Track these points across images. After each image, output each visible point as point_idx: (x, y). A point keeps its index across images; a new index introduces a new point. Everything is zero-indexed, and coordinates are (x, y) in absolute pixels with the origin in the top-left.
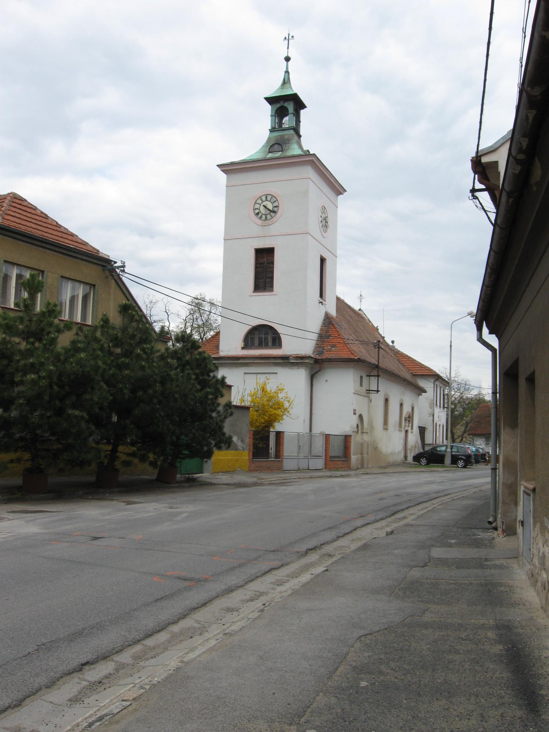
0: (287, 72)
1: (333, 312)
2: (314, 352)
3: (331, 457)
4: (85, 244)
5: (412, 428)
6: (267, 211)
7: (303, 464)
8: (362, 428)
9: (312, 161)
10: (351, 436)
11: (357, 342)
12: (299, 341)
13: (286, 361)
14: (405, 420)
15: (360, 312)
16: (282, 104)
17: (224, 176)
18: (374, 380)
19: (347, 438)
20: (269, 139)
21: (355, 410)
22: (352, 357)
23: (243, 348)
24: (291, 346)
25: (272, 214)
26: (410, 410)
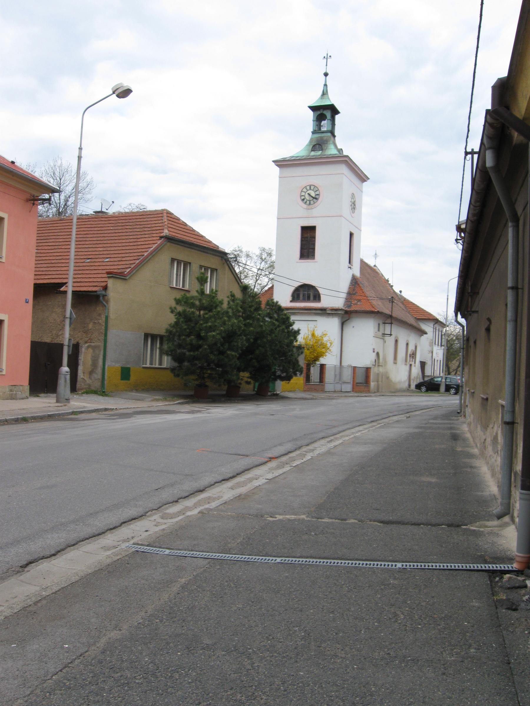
0: (325, 85)
1: (358, 274)
2: (344, 305)
3: (357, 383)
4: (210, 242)
5: (415, 363)
6: (311, 198)
7: (338, 387)
8: (379, 363)
9: (346, 161)
10: (370, 368)
11: (376, 299)
12: (334, 297)
13: (323, 312)
14: (410, 356)
15: (375, 268)
16: (321, 111)
17: (278, 169)
18: (388, 327)
19: (368, 370)
20: (311, 139)
21: (374, 349)
22: (373, 310)
23: (291, 301)
24: (328, 301)
25: (314, 200)
26: (414, 348)
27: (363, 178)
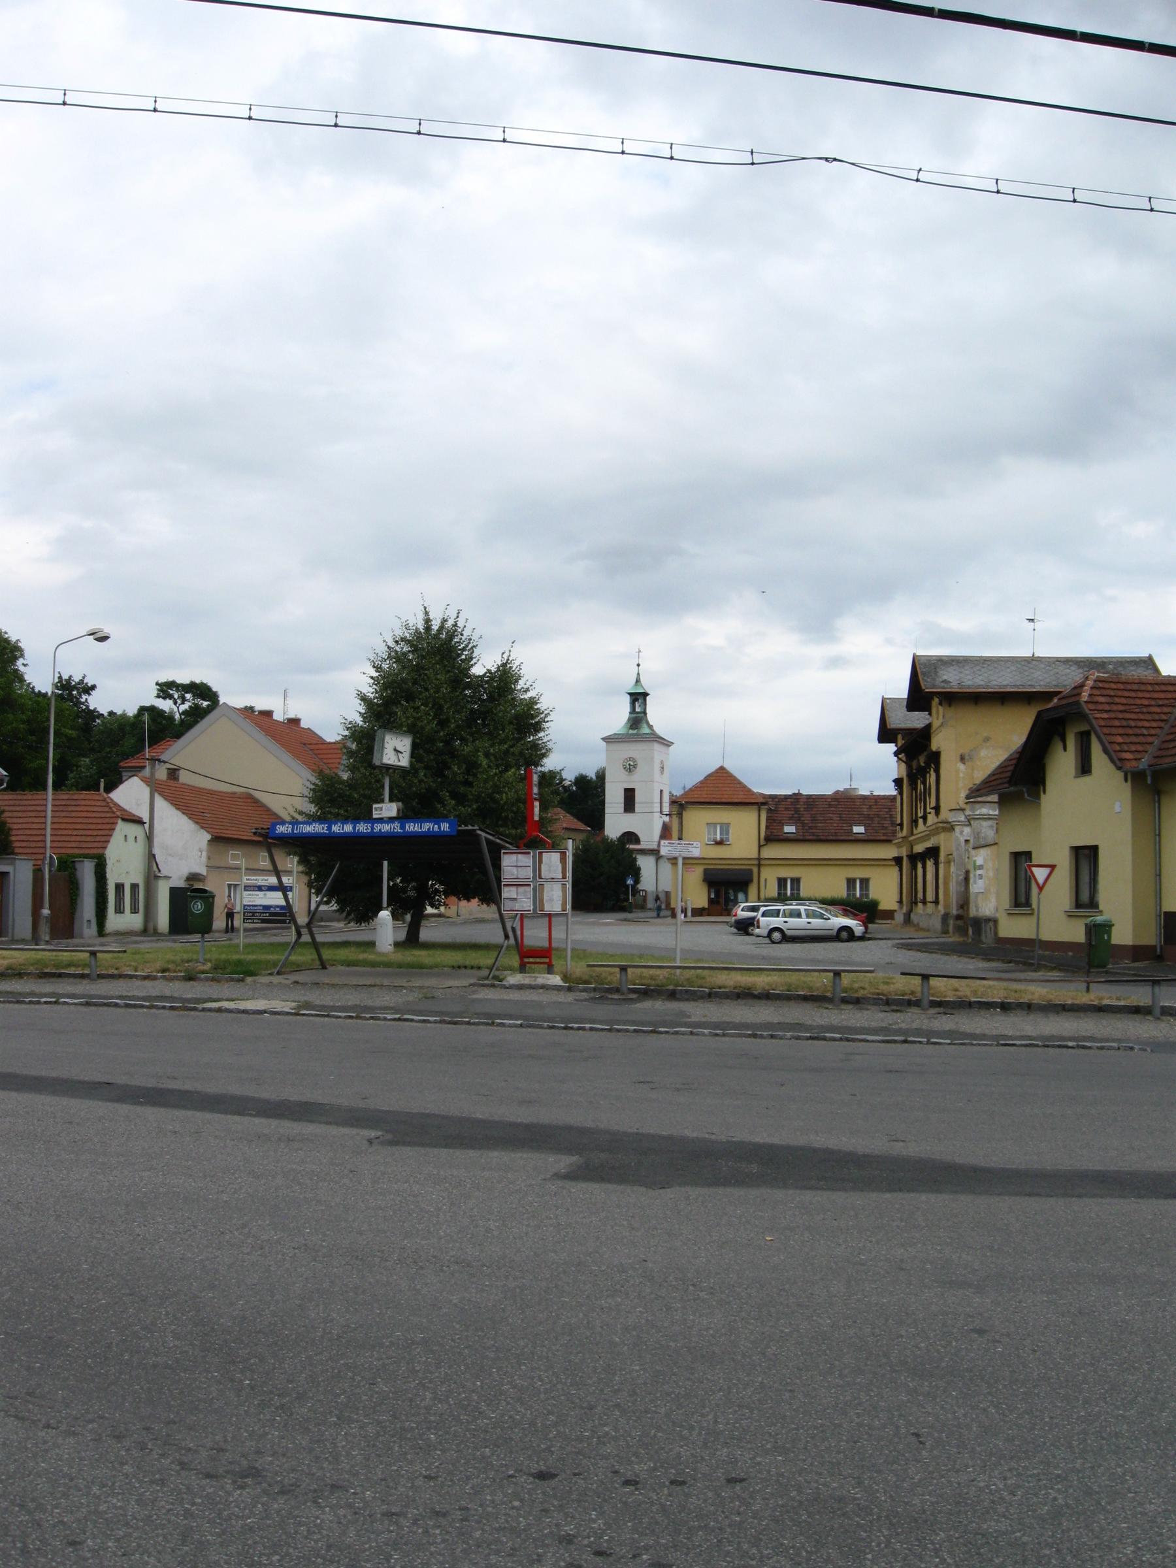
27: (667, 744)
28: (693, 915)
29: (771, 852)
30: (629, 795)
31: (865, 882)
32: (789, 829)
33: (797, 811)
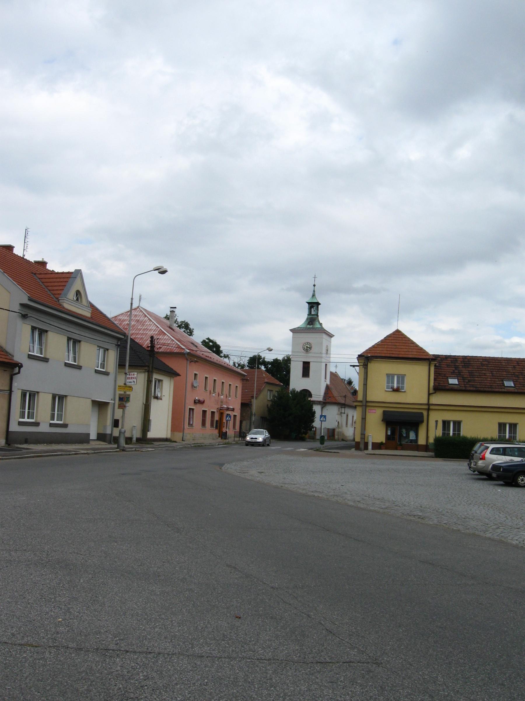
0: (314, 291)
18: (343, 409)
19: (334, 430)
20: (307, 319)
27: (331, 336)
28: (373, 448)
29: (439, 399)
30: (306, 366)
31: (458, 424)
32: (453, 381)
33: (456, 368)
